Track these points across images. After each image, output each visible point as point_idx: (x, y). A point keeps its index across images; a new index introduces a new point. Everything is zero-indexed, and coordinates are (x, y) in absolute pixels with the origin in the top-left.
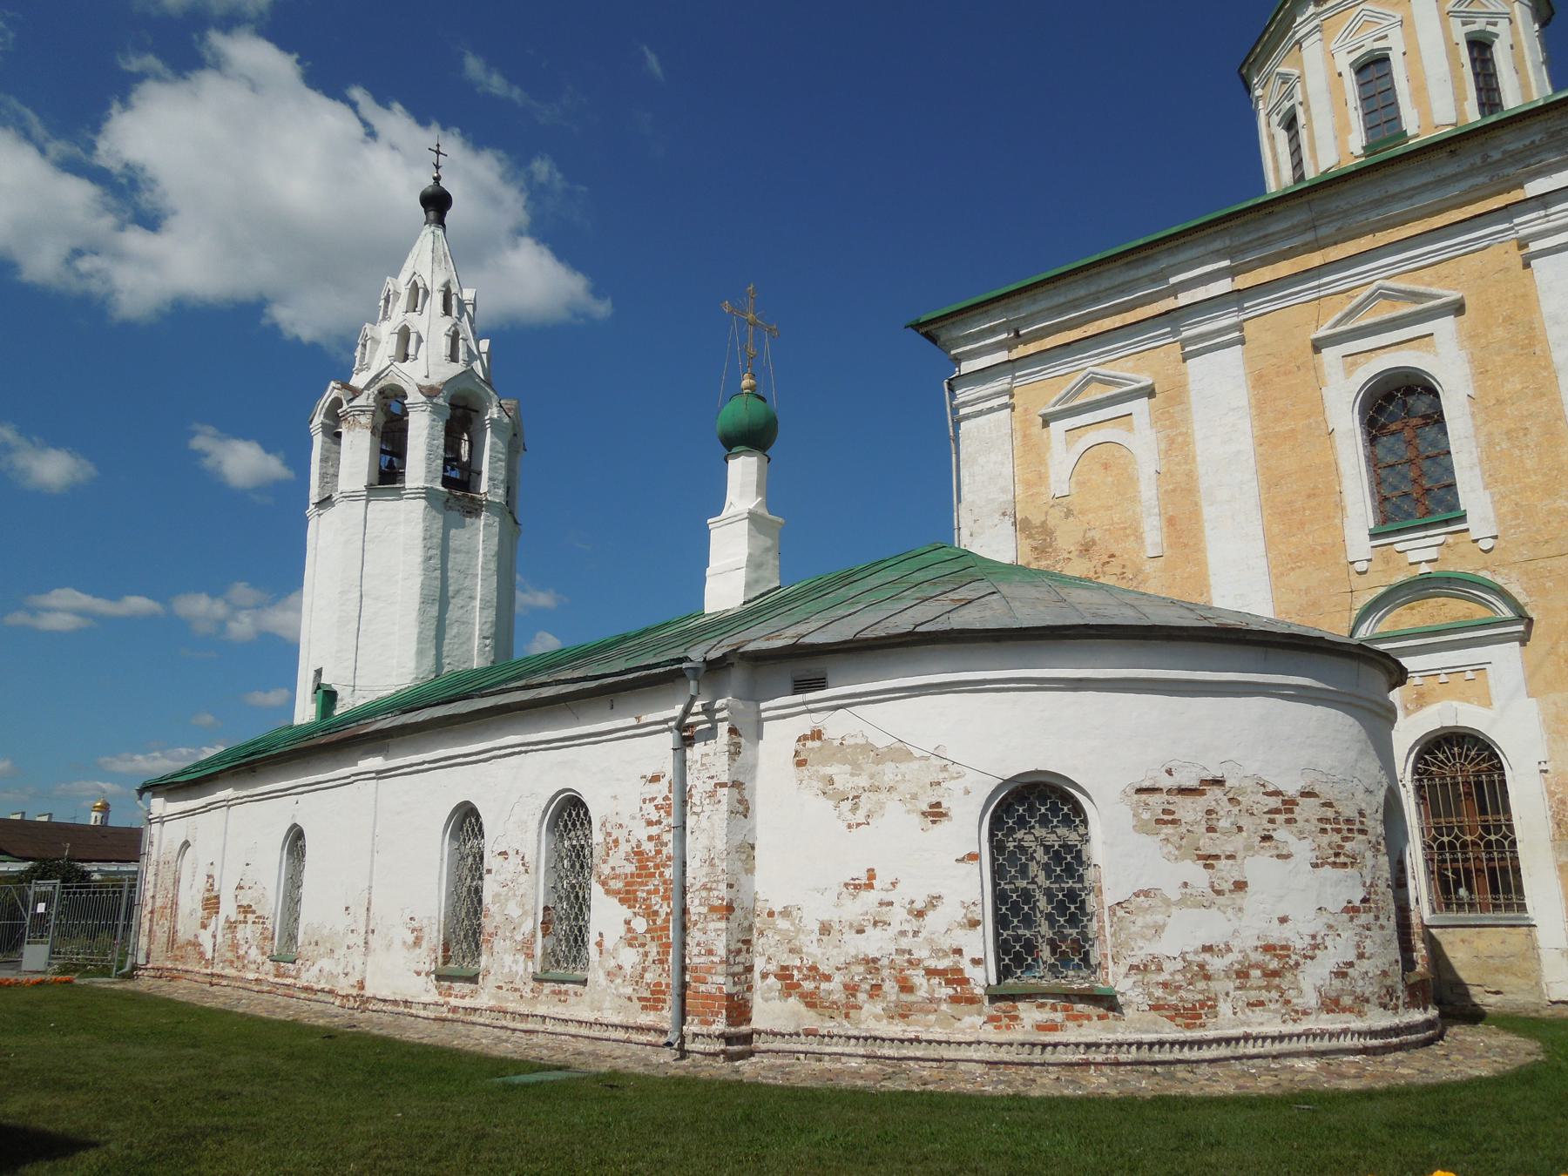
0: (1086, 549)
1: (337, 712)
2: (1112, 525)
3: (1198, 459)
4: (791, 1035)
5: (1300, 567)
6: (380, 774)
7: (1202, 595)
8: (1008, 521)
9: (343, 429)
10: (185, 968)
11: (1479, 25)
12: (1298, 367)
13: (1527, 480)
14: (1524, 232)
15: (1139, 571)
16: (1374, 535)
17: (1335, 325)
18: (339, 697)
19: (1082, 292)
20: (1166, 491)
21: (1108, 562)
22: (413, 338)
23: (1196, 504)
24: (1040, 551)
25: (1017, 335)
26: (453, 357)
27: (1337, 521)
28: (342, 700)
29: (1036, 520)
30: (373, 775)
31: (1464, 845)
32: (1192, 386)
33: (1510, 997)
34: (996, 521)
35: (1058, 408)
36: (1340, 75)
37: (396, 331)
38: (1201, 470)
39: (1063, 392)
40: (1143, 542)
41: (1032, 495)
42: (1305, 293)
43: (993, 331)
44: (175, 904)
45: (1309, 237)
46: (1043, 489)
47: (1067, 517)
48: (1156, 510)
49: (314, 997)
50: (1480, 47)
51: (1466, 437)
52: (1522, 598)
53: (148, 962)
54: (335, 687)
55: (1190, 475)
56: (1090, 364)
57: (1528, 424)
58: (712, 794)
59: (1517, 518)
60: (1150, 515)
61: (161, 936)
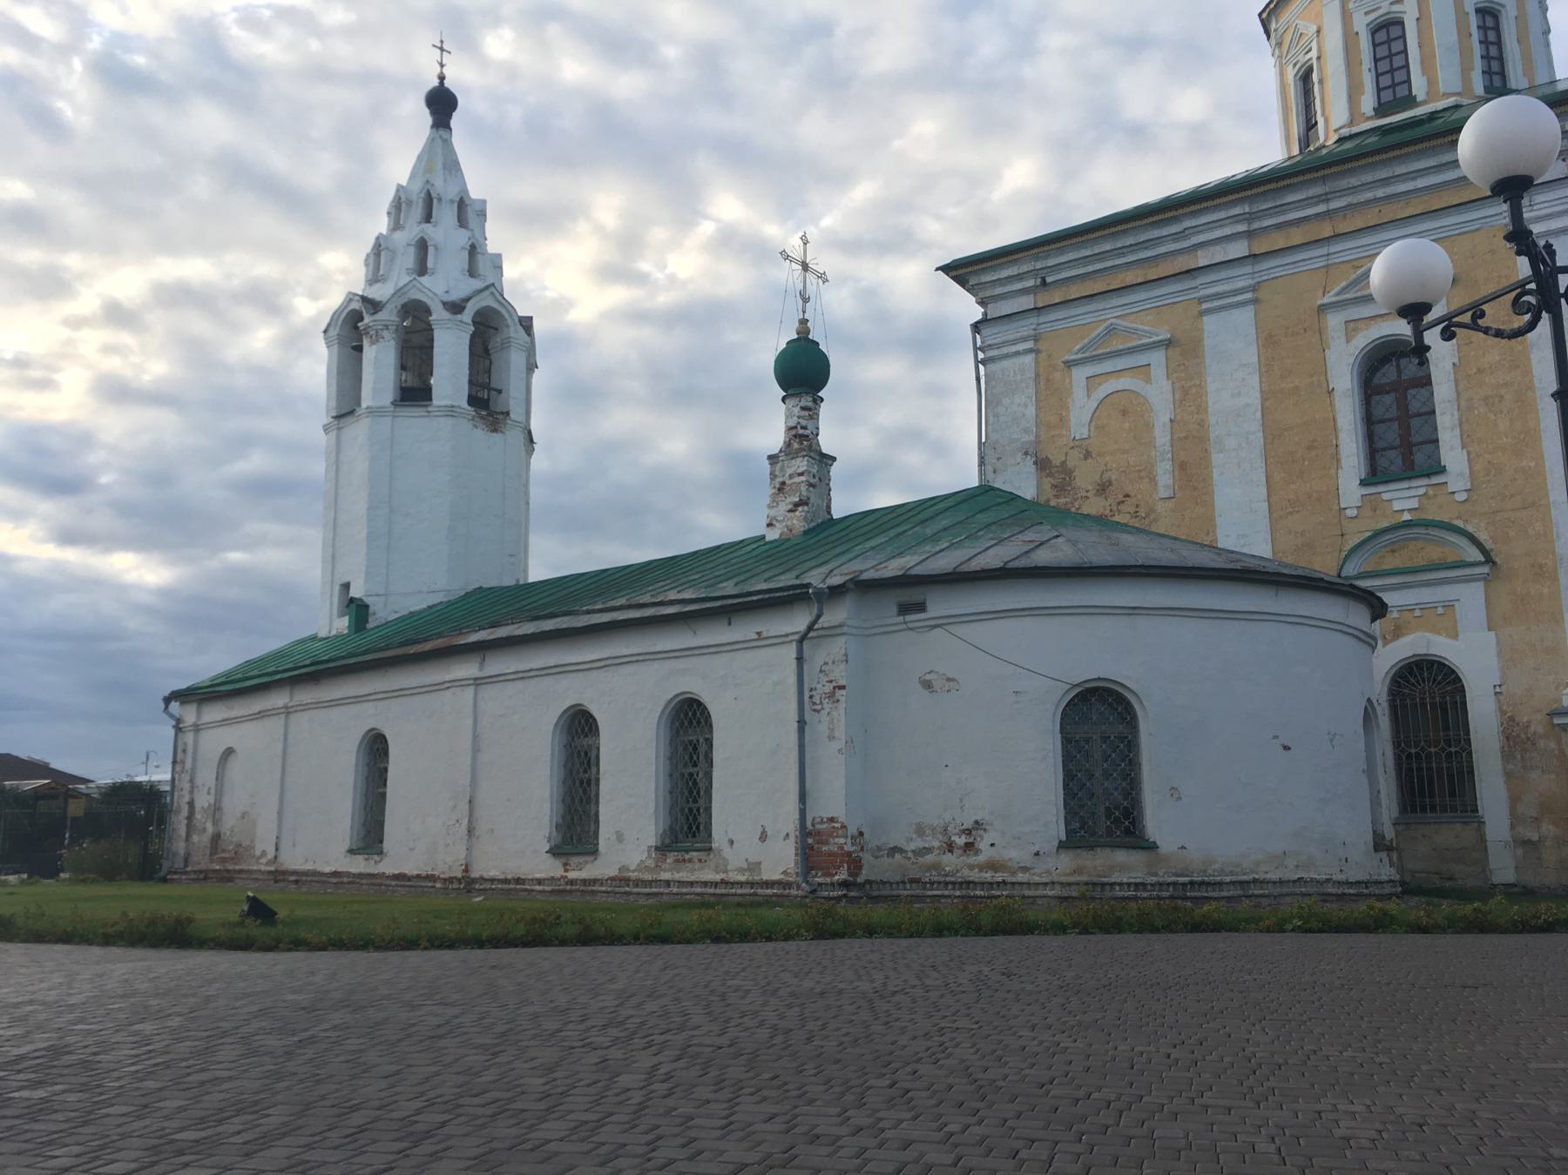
0: (1103, 488)
1: (370, 625)
2: (1127, 467)
3: (1209, 409)
4: (898, 883)
5: (1297, 512)
6: (478, 682)
7: (1208, 534)
8: (1030, 461)
9: (366, 343)
10: (237, 867)
12: (1305, 330)
13: (1500, 442)
15: (1152, 510)
16: (1363, 483)
17: (1338, 294)
18: (371, 610)
20: (1179, 438)
21: (1123, 502)
22: (431, 250)
23: (1206, 451)
24: (1060, 489)
25: (1044, 280)
27: (1333, 471)
28: (374, 614)
29: (1056, 459)
30: (471, 682)
31: (1429, 755)
32: (1206, 342)
33: (1460, 882)
34: (1019, 460)
35: (1080, 356)
36: (1357, 33)
37: (413, 242)
38: (1212, 420)
40: (1156, 485)
41: (1053, 436)
43: (1019, 277)
46: (1064, 432)
47: (1086, 459)
48: (1170, 455)
49: (409, 883)
51: (1449, 401)
52: (1488, 545)
53: (186, 866)
54: (368, 600)
55: (1202, 424)
57: (1503, 392)
58: (831, 695)
59: (1488, 475)
60: (1163, 460)
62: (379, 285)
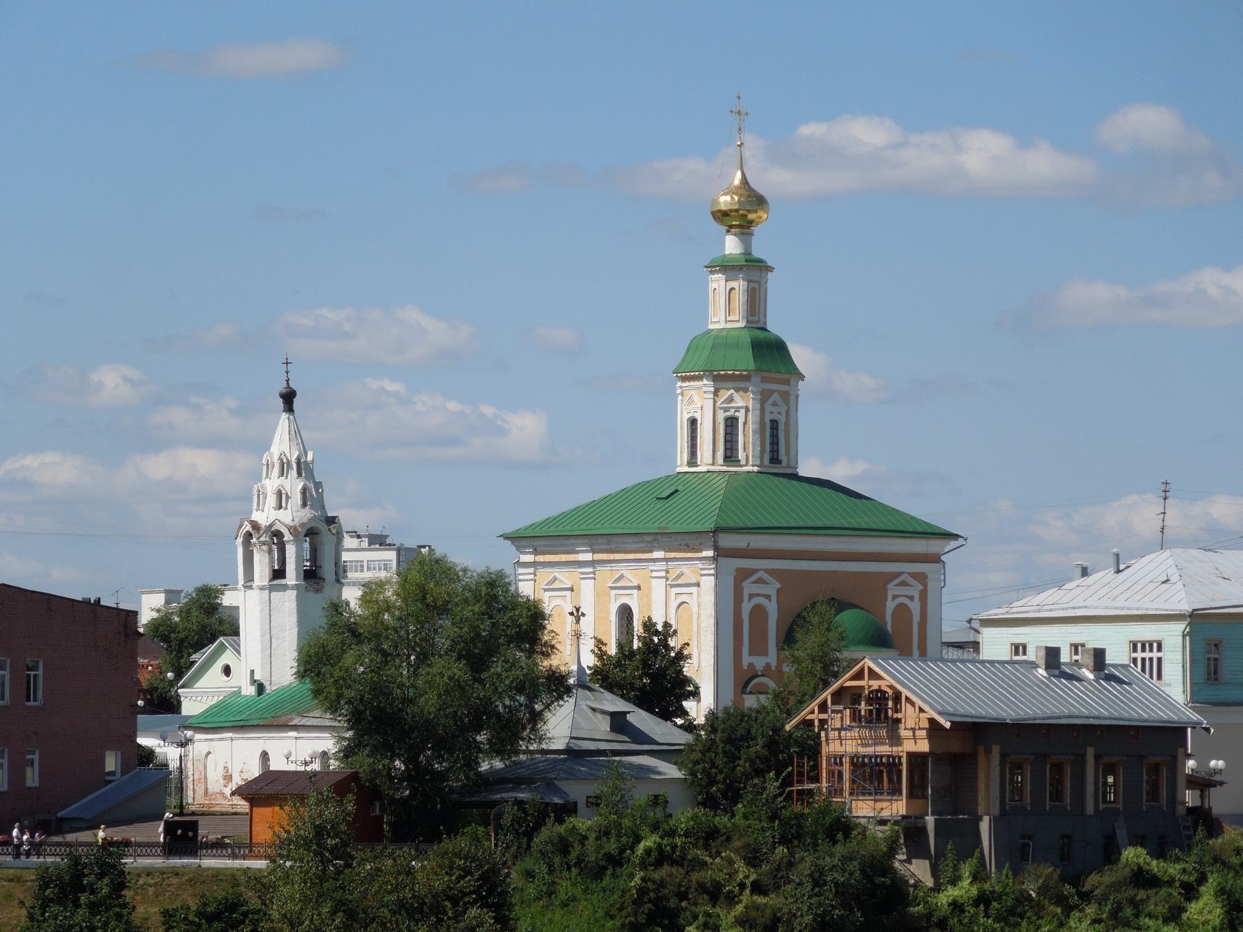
6: (296, 738)
10: (217, 803)
11: (730, 414)
14: (652, 568)
19: (552, 543)
26: (304, 505)
32: (582, 591)
39: (547, 581)
42: (607, 568)
44: (206, 778)
45: (608, 547)
50: (731, 423)
54: (263, 681)
56: (556, 572)
61: (200, 790)
62: (260, 512)
